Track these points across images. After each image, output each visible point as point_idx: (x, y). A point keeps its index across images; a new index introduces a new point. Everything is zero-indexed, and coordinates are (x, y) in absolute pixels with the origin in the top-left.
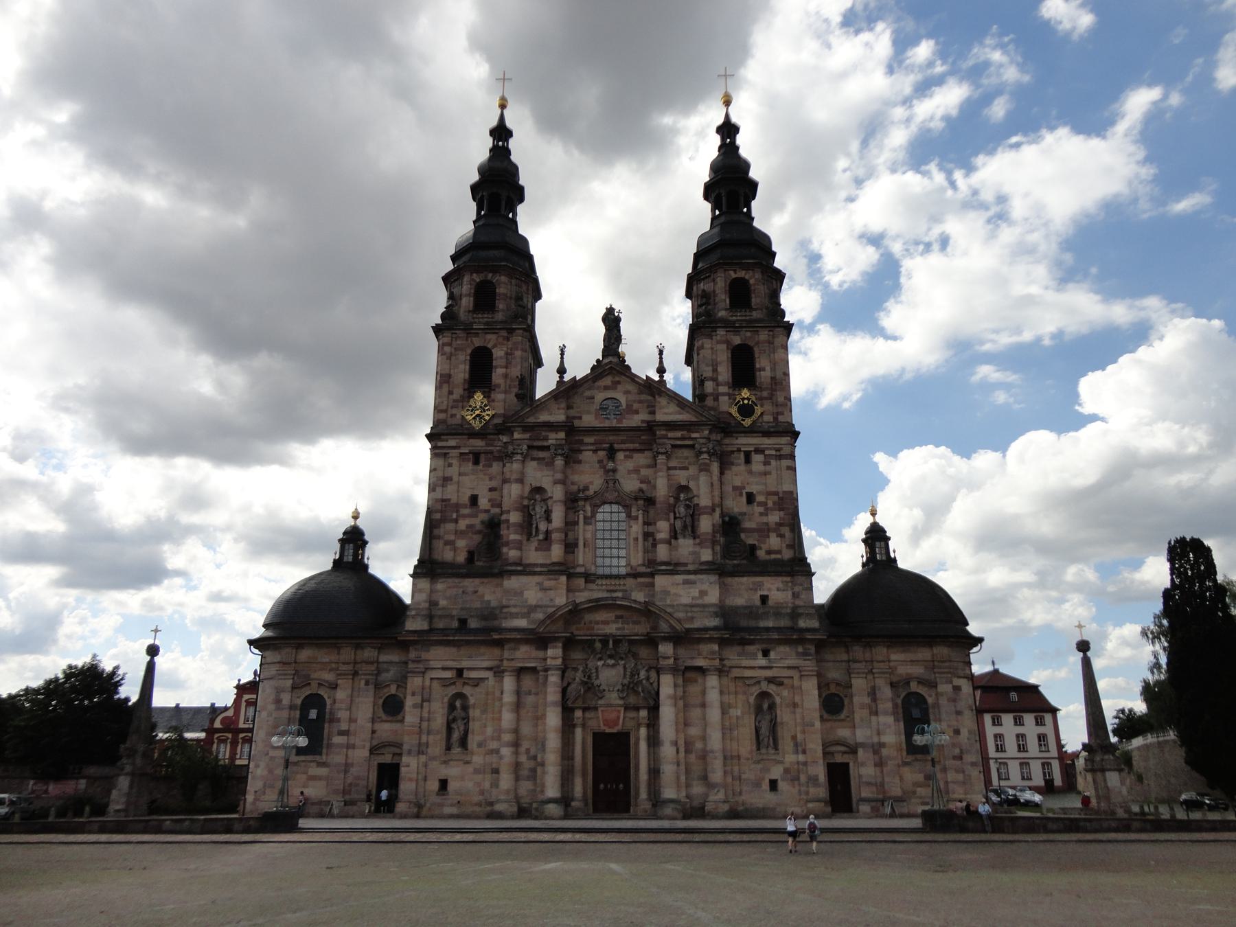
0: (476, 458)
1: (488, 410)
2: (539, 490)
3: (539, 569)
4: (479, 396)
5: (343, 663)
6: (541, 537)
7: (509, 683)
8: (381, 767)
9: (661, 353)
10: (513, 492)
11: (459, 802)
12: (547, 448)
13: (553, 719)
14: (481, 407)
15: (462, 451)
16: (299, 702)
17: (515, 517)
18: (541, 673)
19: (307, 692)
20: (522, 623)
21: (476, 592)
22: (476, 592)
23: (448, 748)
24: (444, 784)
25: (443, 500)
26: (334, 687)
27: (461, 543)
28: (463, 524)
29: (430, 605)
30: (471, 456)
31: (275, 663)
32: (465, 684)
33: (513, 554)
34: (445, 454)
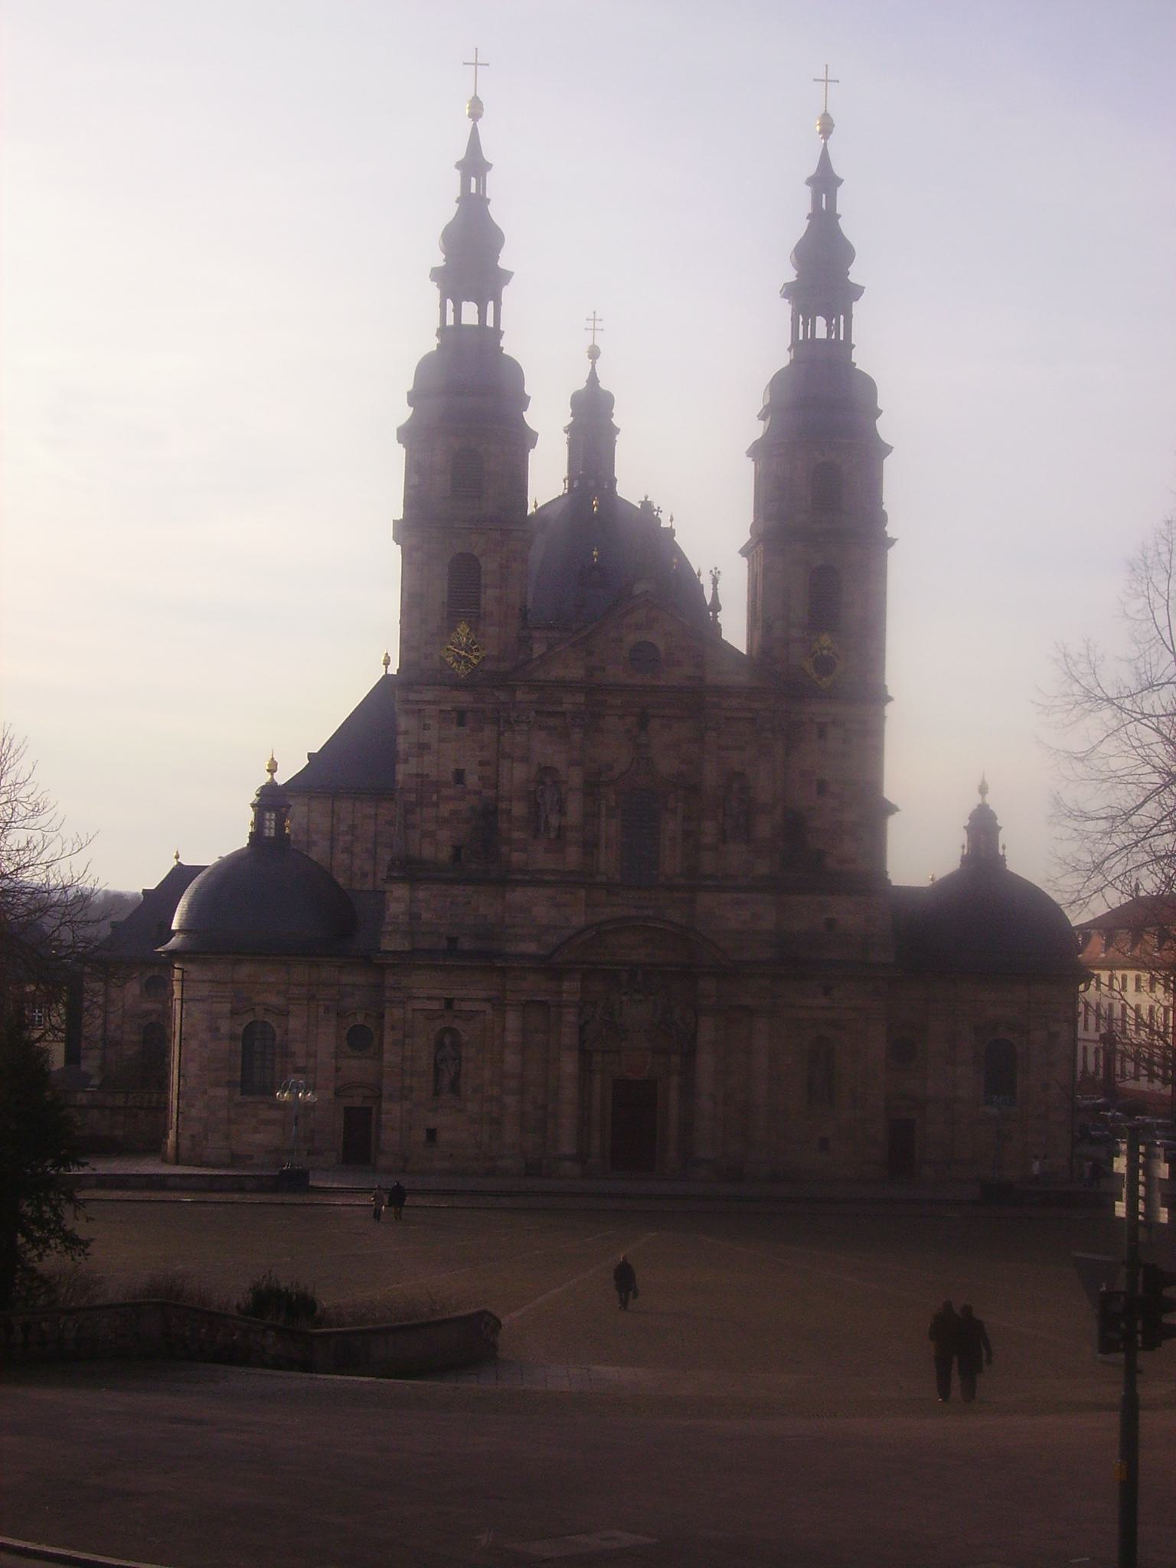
0: (461, 718)
1: (477, 650)
2: (547, 770)
3: (547, 878)
4: (463, 629)
5: (295, 985)
6: (553, 835)
7: (513, 1020)
8: (348, 1111)
9: (715, 582)
10: (518, 773)
11: (451, 1155)
12: (563, 714)
13: (569, 1065)
14: (466, 645)
15: (443, 708)
16: (240, 1030)
17: (519, 809)
18: (552, 1009)
19: (249, 1019)
20: (531, 948)
21: (469, 903)
22: (469, 903)
23: (437, 1093)
24: (432, 1134)
25: (418, 775)
26: (285, 1014)
27: (444, 835)
28: (445, 810)
29: (410, 919)
30: (454, 714)
31: (204, 981)
32: (456, 1016)
33: (517, 857)
34: (420, 710)
